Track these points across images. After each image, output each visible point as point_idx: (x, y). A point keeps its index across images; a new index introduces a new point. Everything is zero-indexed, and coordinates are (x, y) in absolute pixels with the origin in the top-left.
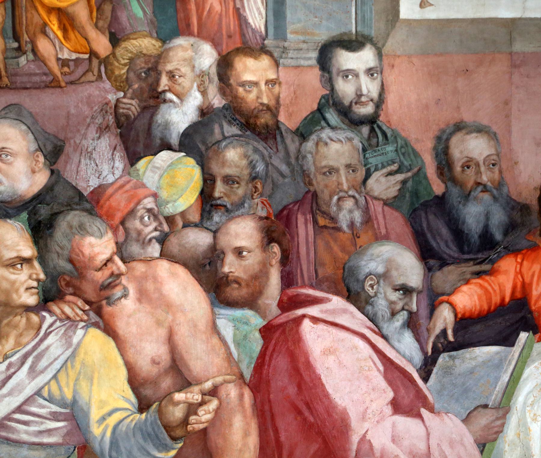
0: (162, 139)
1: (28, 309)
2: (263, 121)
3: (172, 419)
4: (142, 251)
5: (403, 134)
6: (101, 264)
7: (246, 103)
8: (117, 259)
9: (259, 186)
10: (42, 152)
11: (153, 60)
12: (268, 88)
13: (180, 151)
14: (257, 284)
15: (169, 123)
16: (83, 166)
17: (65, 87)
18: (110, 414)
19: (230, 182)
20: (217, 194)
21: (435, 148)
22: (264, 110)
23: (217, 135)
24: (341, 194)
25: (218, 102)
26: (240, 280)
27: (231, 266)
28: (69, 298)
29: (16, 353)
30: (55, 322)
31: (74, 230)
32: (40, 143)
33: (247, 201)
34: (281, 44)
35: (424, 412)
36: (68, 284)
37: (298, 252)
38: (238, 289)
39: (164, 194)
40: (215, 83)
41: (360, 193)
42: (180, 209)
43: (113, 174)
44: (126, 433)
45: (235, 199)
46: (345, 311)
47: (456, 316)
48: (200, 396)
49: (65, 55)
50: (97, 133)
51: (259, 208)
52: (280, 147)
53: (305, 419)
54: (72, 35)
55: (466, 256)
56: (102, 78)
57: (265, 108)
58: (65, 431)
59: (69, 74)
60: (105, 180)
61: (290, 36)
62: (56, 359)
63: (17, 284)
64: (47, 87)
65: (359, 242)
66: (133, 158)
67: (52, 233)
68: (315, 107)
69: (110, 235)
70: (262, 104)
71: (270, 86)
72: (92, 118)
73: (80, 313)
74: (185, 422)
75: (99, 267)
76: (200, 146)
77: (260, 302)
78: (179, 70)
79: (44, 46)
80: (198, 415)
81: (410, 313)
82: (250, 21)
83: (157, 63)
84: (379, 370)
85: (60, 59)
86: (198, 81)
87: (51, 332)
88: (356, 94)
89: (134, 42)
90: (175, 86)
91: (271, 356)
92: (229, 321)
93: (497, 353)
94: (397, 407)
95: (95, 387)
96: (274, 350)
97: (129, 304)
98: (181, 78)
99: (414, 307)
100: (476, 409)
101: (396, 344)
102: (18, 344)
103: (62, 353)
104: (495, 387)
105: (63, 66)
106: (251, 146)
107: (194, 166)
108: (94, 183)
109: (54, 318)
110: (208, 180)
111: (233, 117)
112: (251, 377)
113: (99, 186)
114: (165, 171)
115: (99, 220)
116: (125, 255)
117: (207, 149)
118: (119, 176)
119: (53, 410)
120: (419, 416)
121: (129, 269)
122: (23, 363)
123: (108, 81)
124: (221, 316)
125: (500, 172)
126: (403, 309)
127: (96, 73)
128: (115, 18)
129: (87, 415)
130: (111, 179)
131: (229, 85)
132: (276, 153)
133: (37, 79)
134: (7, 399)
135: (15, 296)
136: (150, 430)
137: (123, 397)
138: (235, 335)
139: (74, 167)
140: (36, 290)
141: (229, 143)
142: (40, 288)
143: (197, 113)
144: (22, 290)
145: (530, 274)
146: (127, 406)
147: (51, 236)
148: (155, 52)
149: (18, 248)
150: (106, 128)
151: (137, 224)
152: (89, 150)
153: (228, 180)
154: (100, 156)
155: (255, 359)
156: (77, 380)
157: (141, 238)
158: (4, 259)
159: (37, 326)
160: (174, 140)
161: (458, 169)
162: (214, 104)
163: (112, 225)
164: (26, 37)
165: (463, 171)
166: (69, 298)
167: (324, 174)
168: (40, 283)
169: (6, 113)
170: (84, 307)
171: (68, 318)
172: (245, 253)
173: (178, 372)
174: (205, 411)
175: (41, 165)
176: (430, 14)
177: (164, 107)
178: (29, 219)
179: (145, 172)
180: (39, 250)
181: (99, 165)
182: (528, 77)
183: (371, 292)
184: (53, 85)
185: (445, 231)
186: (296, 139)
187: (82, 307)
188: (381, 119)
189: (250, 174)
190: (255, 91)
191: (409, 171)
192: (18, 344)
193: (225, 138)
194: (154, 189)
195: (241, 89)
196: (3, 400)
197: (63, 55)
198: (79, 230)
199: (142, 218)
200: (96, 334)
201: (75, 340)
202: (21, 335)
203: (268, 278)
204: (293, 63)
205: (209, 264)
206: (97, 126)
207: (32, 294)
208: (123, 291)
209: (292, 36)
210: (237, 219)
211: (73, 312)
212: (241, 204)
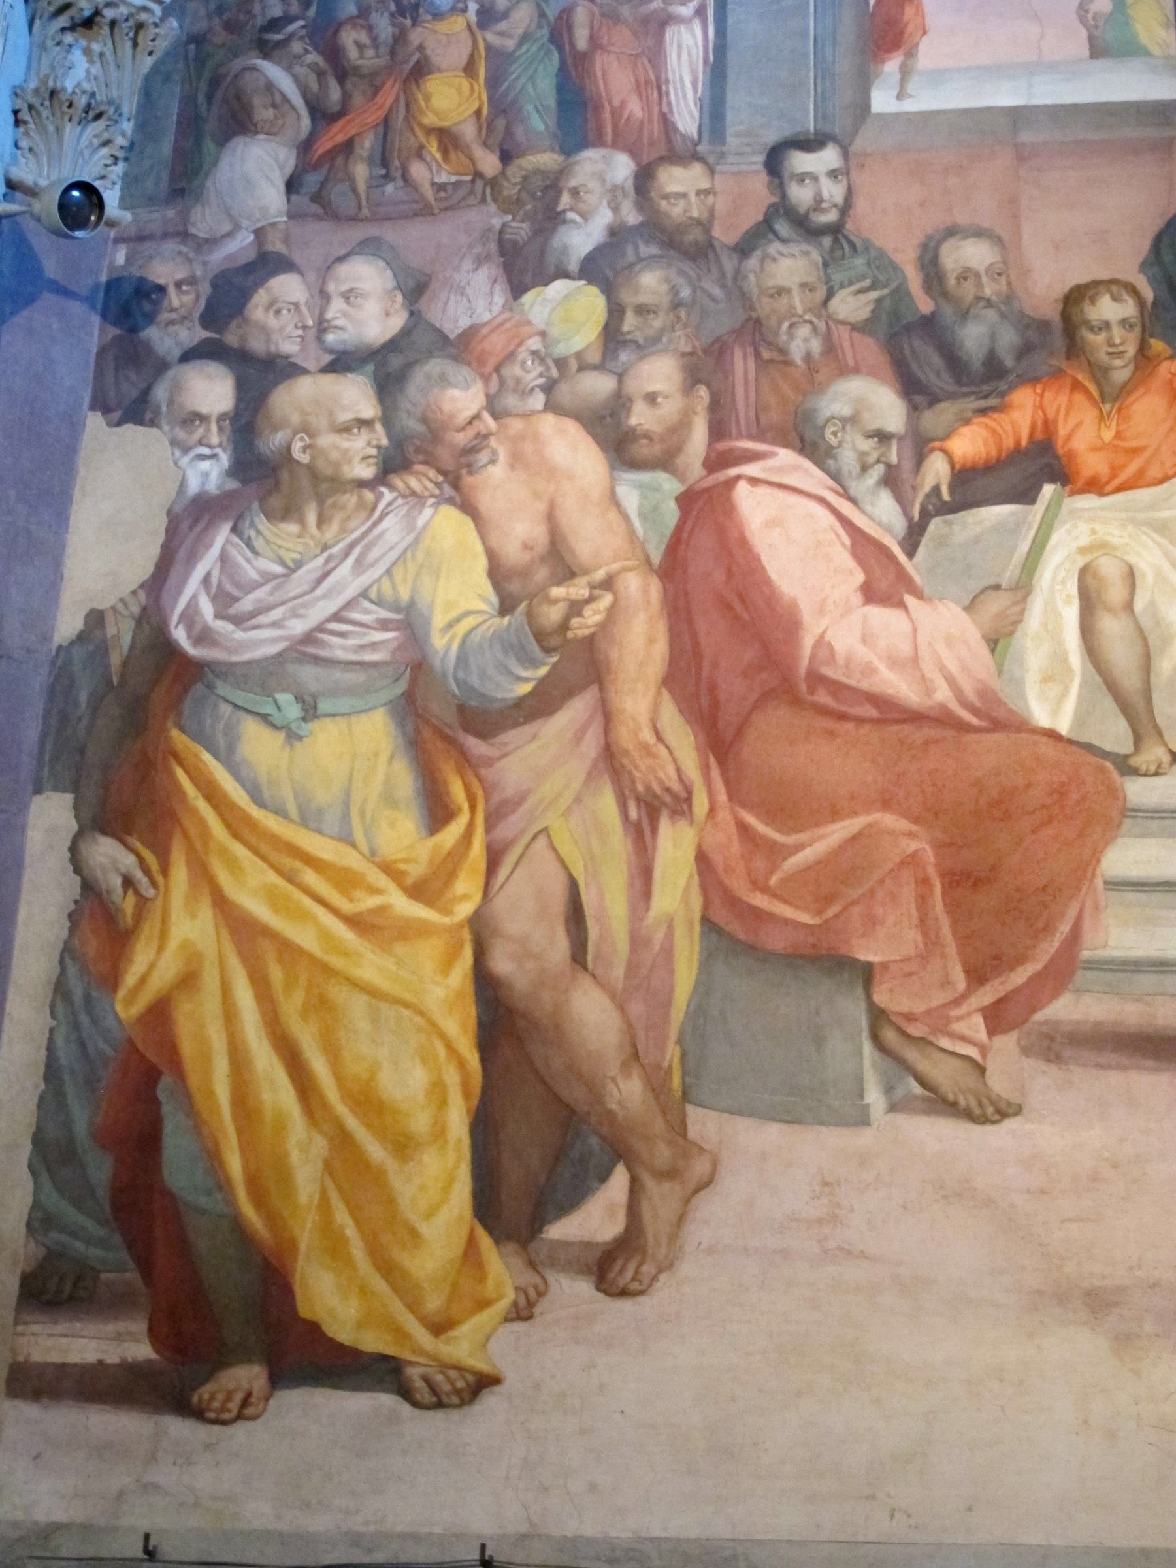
0: (557, 267)
1: (361, 484)
5: (878, 244)
7: (669, 217)
8: (486, 416)
9: (683, 314)
13: (580, 278)
16: (451, 303)
18: (458, 620)
20: (626, 328)
21: (921, 259)
23: (630, 256)
24: (795, 319)
25: (632, 217)
27: (640, 417)
28: (418, 467)
29: (339, 542)
30: (396, 498)
34: (718, 149)
35: (909, 599)
36: (418, 450)
37: (733, 393)
39: (554, 332)
41: (819, 317)
43: (490, 311)
45: (651, 332)
46: (796, 468)
47: (953, 468)
49: (443, 178)
53: (737, 618)
54: (453, 156)
55: (965, 390)
58: (396, 643)
61: (729, 139)
62: (392, 548)
64: (416, 215)
65: (819, 377)
66: (517, 290)
68: (761, 217)
70: (691, 218)
73: (430, 486)
74: (564, 626)
79: (418, 171)
81: (889, 466)
82: (680, 125)
84: (843, 544)
87: (387, 514)
88: (815, 200)
89: (530, 158)
91: (692, 530)
93: (1013, 514)
94: (870, 594)
97: (497, 472)
99: (894, 459)
100: (982, 592)
101: (868, 508)
102: (343, 530)
104: (1010, 560)
105: (438, 191)
106: (674, 268)
108: (464, 323)
110: (615, 312)
115: (467, 368)
120: (902, 605)
121: (500, 426)
125: (1009, 283)
126: (878, 461)
127: (479, 195)
128: (508, 132)
129: (427, 621)
130: (486, 317)
131: (649, 199)
133: (405, 207)
134: (321, 603)
138: (641, 506)
143: (605, 233)
144: (357, 459)
145: (1055, 407)
146: (483, 606)
147: (401, 391)
148: (557, 167)
153: (642, 310)
156: (418, 574)
160: (573, 266)
161: (952, 281)
164: (397, 163)
165: (959, 283)
166: (418, 467)
167: (772, 296)
171: (413, 493)
172: (659, 400)
173: (559, 559)
175: (398, 306)
176: (910, 106)
177: (562, 229)
178: (375, 373)
179: (532, 306)
181: (473, 299)
182: (1039, 170)
183: (834, 441)
185: (937, 361)
186: (735, 256)
188: (847, 226)
191: (886, 287)
192: (343, 530)
193: (640, 260)
195: (664, 204)
199: (523, 363)
201: (421, 521)
202: (349, 518)
204: (734, 169)
205: (611, 416)
207: (369, 465)
209: (733, 139)
212: (656, 339)
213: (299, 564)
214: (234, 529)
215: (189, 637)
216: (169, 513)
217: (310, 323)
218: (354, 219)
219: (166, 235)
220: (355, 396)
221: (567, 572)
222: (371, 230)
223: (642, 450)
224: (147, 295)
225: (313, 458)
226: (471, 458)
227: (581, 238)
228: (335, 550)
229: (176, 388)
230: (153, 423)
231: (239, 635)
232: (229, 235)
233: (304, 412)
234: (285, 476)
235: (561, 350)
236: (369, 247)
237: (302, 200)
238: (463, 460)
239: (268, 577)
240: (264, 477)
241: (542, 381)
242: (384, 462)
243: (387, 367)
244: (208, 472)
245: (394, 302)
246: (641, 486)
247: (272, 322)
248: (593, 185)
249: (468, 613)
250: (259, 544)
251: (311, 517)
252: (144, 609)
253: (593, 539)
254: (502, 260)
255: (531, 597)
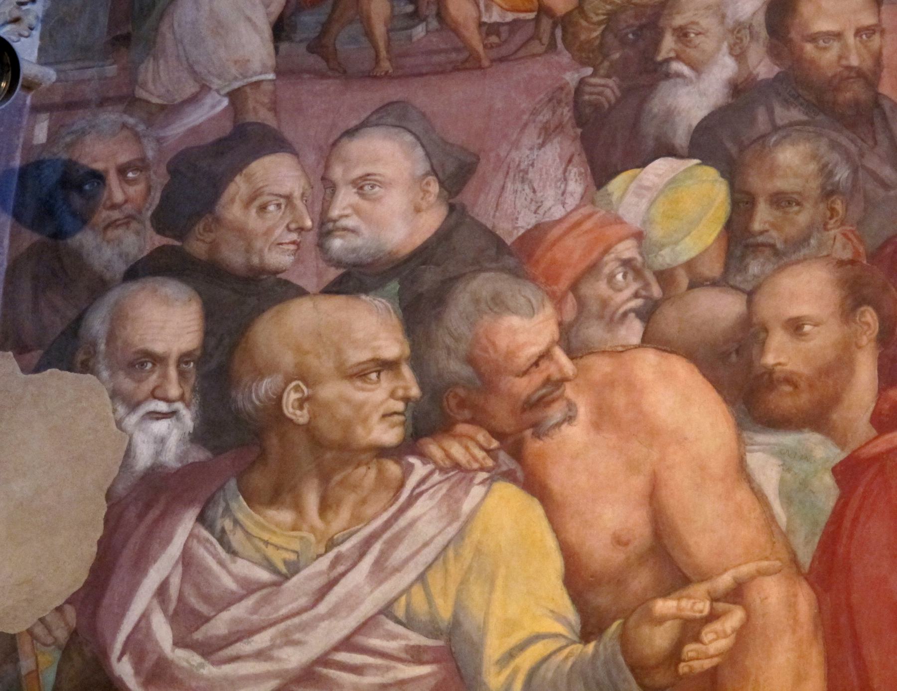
0: (657, 139)
1: (382, 452)
2: (849, 95)
3: (648, 651)
4: (608, 336)
6: (528, 364)
8: (560, 355)
9: (839, 206)
10: (437, 175)
11: (649, 12)
12: (861, 42)
13: (690, 156)
14: (831, 383)
15: (673, 111)
16: (508, 195)
17: (490, 67)
18: (522, 647)
19: (783, 204)
20: (757, 226)
22: (852, 78)
25: (764, 68)
26: (795, 378)
27: (779, 353)
29: (351, 535)
30: (431, 473)
31: (483, 306)
32: (434, 161)
33: (815, 234)
36: (462, 404)
38: (791, 394)
39: (656, 233)
40: (761, 41)
42: (684, 258)
43: (564, 204)
44: (554, 684)
45: (791, 231)
48: (708, 603)
49: (495, 16)
50: (539, 137)
51: (838, 245)
52: (881, 137)
56: (556, 47)
57: (853, 74)
58: (432, 682)
59: (499, 46)
60: (547, 215)
62: (426, 545)
63: (367, 409)
64: (456, 69)
66: (601, 174)
67: (439, 313)
69: (549, 309)
70: (849, 68)
71: (864, 37)
72: (532, 114)
73: (480, 454)
74: (675, 655)
75: (524, 369)
76: (729, 145)
77: (835, 416)
78: (697, 23)
80: (701, 642)
83: (658, 15)
85: (485, 23)
86: (731, 39)
87: (421, 494)
90: (688, 50)
91: (855, 520)
92: (773, 454)
95: (498, 595)
96: (860, 508)
97: (575, 434)
98: (700, 36)
102: (357, 519)
103: (440, 533)
105: (488, 34)
107: (716, 181)
108: (526, 221)
109: (430, 467)
110: (742, 203)
111: (793, 92)
112: (813, 562)
113: (537, 226)
114: (662, 192)
115: (531, 285)
116: (575, 343)
117: (741, 151)
118: (572, 208)
119: (412, 643)
121: (581, 371)
122: (362, 555)
123: (566, 52)
124: (756, 447)
127: (546, 39)
129: (477, 649)
130: (558, 213)
132: (873, 148)
133: (441, 58)
134: (324, 624)
135: (360, 431)
136: (601, 673)
137: (552, 611)
138: (782, 482)
139: (492, 197)
140: (401, 418)
141: (784, 137)
142: (409, 414)
143: (726, 91)
144: (376, 417)
146: (559, 628)
147: (438, 318)
149: (376, 344)
150: (557, 127)
151: (602, 288)
152: (523, 167)
153: (780, 200)
154: (541, 175)
155: (822, 525)
156: (464, 582)
157: (607, 313)
158: (348, 364)
159: (395, 484)
160: (681, 138)
162: (758, 75)
163: (554, 293)
168: (411, 404)
169: (382, 117)
170: (490, 443)
171: (457, 466)
172: (807, 328)
173: (666, 558)
174: (716, 633)
175: (432, 199)
178: (400, 294)
180: (414, 346)
181: (539, 188)
184: (467, 65)
187: (485, 445)
189: (823, 187)
190: (835, 48)
193: (776, 128)
194: (638, 225)
195: (809, 47)
196: (317, 627)
197: (490, 17)
198: (492, 306)
199: (611, 277)
200: (507, 491)
201: (467, 506)
202: (364, 502)
203: (852, 372)
205: (737, 352)
206: (540, 125)
207: (393, 426)
208: (566, 409)
210: (794, 267)
211: (468, 455)
212: (803, 240)
213: (294, 568)
214: (201, 519)
215: (137, 673)
216: (108, 497)
217: (308, 223)
218: (371, 76)
219: (103, 102)
220: (372, 327)
221: (677, 576)
222: (393, 92)
223: (783, 401)
224: (80, 189)
225: (313, 416)
226: (537, 415)
227: (692, 99)
228: (345, 548)
229: (118, 319)
230: (86, 368)
231: (209, 670)
232: (194, 100)
233: (299, 350)
234: (273, 441)
235: (666, 258)
236: (392, 116)
237: (297, 50)
238: (529, 416)
239: (250, 587)
240: (246, 443)
241: (637, 303)
242: (415, 418)
243: (418, 285)
244: (163, 437)
245: (426, 192)
246: (781, 453)
247: (253, 221)
248: (708, 22)
249: (537, 638)
250: (236, 539)
251: (311, 500)
252: (74, 634)
253: (714, 528)
254: (579, 131)
255: (626, 614)
